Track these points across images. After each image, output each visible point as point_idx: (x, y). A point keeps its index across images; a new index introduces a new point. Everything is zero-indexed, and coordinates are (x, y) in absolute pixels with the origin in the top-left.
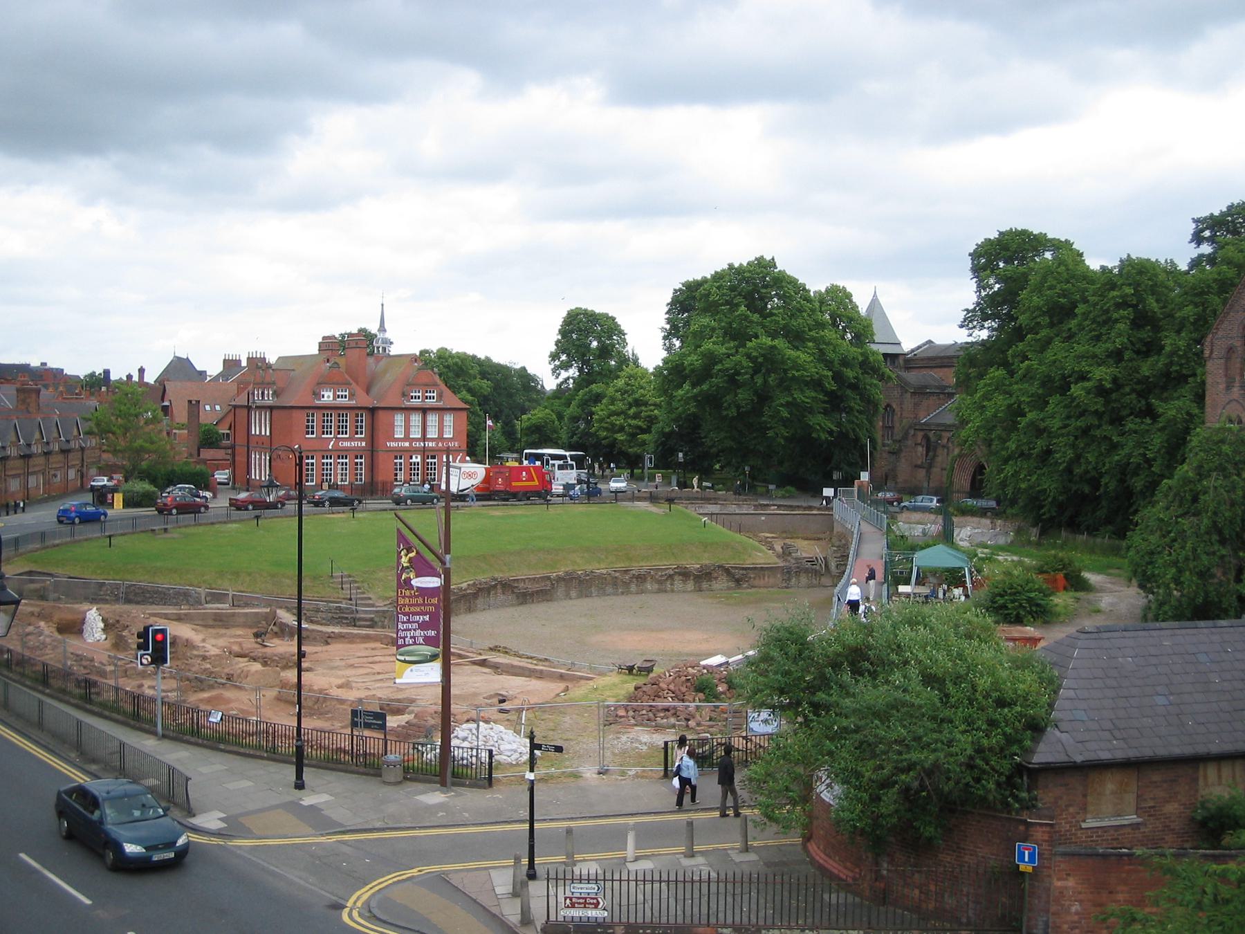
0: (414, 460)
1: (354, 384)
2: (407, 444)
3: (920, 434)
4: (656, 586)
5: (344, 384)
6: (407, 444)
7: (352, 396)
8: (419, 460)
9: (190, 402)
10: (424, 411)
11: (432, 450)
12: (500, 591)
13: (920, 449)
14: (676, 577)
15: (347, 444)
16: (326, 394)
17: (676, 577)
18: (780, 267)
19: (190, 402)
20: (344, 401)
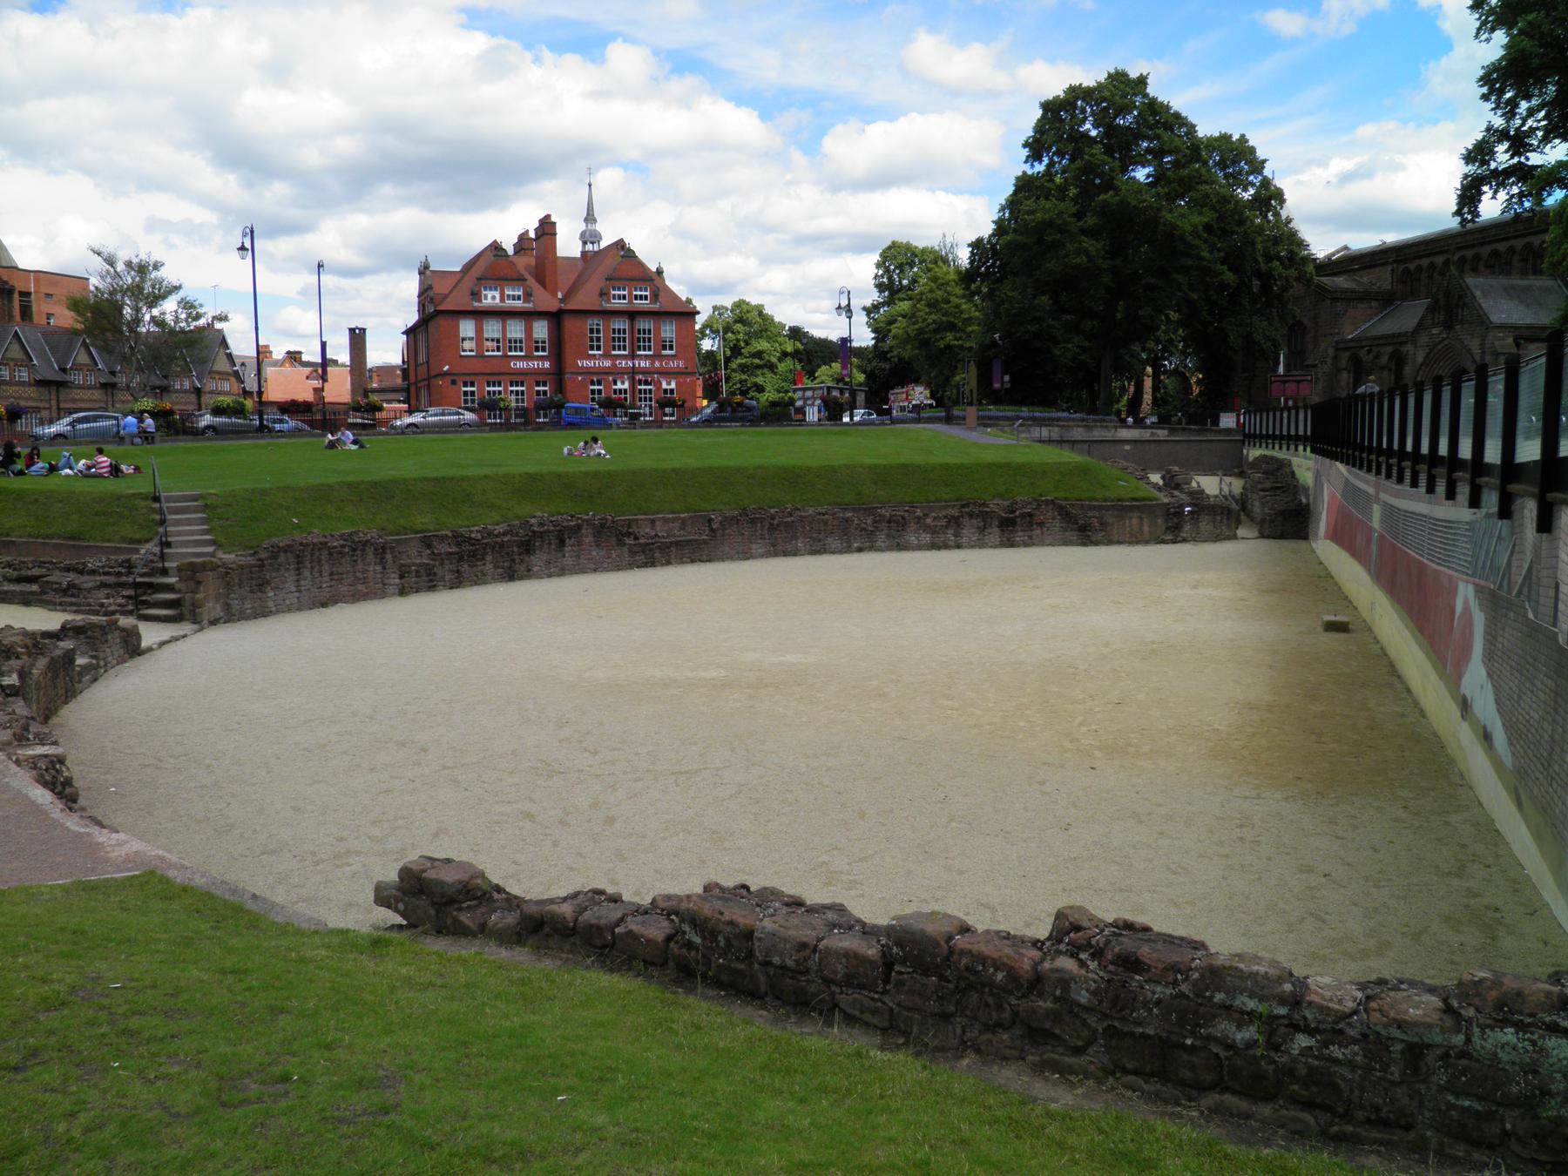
0: (619, 386)
1: (532, 282)
2: (607, 363)
3: (1345, 356)
4: (926, 538)
5: (518, 280)
6: (607, 363)
7: (528, 296)
8: (626, 386)
9: (352, 331)
10: (632, 315)
11: (644, 372)
12: (590, 538)
13: (1345, 375)
14: (965, 521)
15: (520, 365)
16: (490, 294)
17: (965, 521)
18: (1152, 90)
19: (352, 331)
20: (519, 304)
